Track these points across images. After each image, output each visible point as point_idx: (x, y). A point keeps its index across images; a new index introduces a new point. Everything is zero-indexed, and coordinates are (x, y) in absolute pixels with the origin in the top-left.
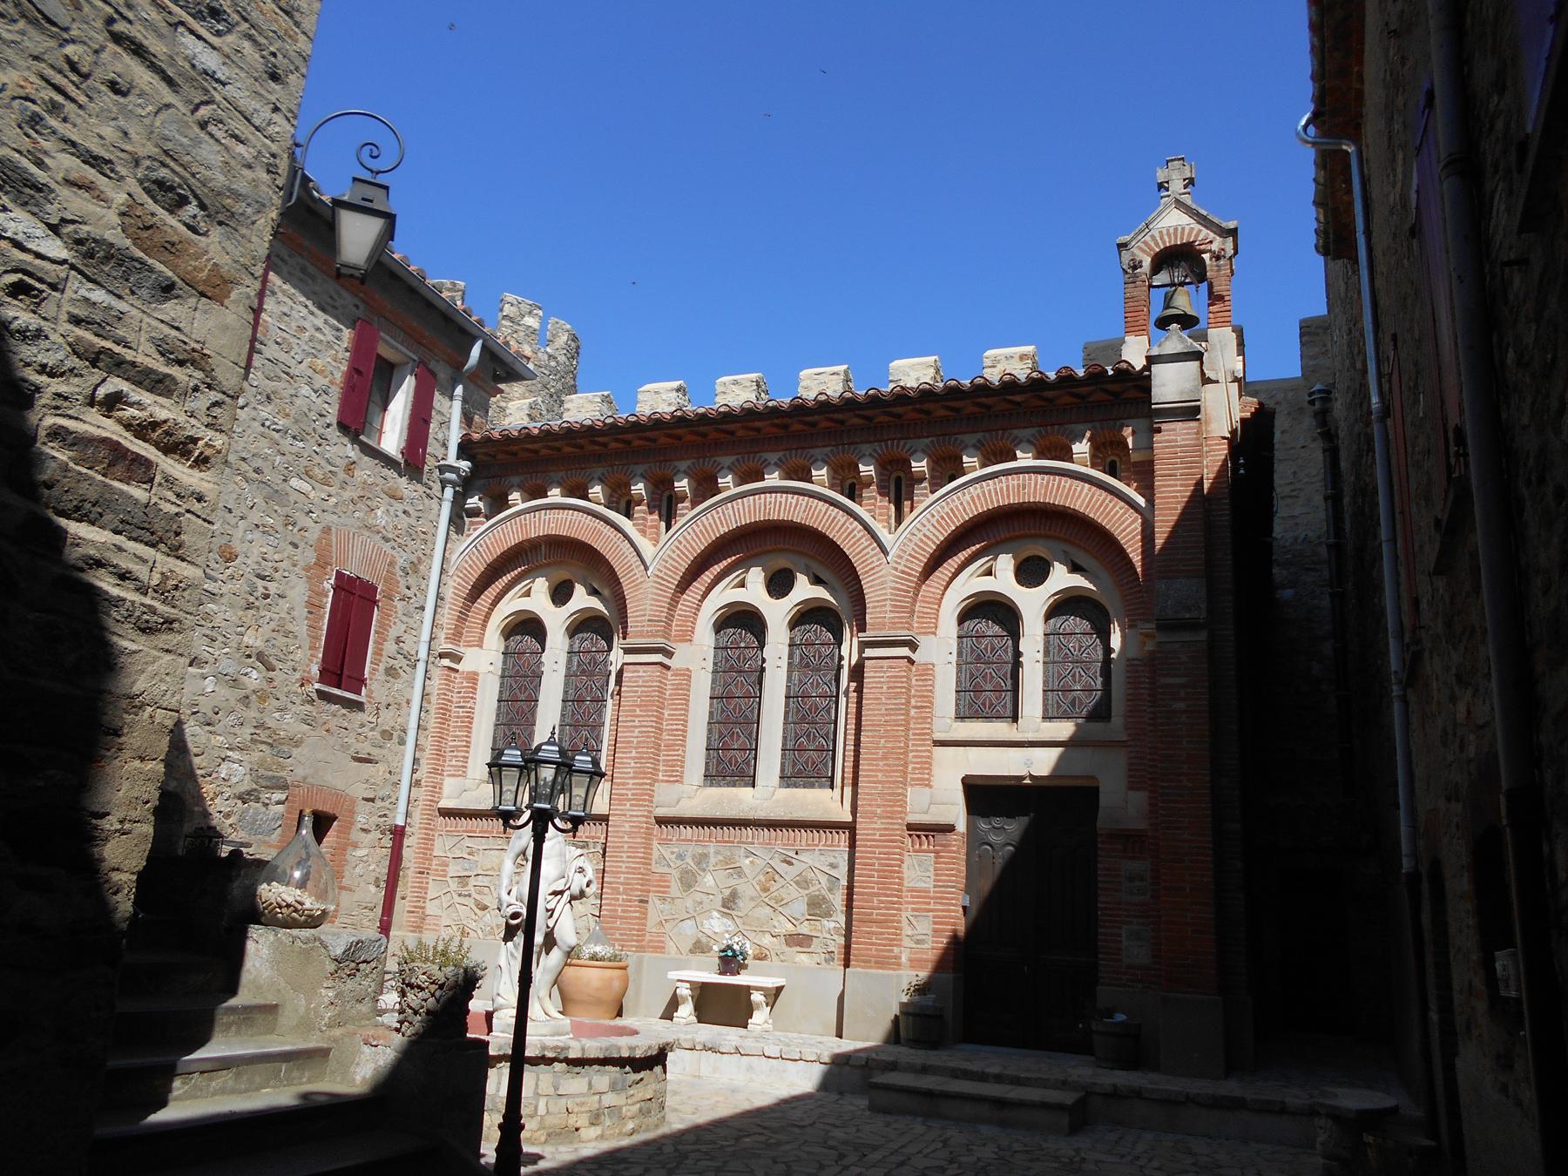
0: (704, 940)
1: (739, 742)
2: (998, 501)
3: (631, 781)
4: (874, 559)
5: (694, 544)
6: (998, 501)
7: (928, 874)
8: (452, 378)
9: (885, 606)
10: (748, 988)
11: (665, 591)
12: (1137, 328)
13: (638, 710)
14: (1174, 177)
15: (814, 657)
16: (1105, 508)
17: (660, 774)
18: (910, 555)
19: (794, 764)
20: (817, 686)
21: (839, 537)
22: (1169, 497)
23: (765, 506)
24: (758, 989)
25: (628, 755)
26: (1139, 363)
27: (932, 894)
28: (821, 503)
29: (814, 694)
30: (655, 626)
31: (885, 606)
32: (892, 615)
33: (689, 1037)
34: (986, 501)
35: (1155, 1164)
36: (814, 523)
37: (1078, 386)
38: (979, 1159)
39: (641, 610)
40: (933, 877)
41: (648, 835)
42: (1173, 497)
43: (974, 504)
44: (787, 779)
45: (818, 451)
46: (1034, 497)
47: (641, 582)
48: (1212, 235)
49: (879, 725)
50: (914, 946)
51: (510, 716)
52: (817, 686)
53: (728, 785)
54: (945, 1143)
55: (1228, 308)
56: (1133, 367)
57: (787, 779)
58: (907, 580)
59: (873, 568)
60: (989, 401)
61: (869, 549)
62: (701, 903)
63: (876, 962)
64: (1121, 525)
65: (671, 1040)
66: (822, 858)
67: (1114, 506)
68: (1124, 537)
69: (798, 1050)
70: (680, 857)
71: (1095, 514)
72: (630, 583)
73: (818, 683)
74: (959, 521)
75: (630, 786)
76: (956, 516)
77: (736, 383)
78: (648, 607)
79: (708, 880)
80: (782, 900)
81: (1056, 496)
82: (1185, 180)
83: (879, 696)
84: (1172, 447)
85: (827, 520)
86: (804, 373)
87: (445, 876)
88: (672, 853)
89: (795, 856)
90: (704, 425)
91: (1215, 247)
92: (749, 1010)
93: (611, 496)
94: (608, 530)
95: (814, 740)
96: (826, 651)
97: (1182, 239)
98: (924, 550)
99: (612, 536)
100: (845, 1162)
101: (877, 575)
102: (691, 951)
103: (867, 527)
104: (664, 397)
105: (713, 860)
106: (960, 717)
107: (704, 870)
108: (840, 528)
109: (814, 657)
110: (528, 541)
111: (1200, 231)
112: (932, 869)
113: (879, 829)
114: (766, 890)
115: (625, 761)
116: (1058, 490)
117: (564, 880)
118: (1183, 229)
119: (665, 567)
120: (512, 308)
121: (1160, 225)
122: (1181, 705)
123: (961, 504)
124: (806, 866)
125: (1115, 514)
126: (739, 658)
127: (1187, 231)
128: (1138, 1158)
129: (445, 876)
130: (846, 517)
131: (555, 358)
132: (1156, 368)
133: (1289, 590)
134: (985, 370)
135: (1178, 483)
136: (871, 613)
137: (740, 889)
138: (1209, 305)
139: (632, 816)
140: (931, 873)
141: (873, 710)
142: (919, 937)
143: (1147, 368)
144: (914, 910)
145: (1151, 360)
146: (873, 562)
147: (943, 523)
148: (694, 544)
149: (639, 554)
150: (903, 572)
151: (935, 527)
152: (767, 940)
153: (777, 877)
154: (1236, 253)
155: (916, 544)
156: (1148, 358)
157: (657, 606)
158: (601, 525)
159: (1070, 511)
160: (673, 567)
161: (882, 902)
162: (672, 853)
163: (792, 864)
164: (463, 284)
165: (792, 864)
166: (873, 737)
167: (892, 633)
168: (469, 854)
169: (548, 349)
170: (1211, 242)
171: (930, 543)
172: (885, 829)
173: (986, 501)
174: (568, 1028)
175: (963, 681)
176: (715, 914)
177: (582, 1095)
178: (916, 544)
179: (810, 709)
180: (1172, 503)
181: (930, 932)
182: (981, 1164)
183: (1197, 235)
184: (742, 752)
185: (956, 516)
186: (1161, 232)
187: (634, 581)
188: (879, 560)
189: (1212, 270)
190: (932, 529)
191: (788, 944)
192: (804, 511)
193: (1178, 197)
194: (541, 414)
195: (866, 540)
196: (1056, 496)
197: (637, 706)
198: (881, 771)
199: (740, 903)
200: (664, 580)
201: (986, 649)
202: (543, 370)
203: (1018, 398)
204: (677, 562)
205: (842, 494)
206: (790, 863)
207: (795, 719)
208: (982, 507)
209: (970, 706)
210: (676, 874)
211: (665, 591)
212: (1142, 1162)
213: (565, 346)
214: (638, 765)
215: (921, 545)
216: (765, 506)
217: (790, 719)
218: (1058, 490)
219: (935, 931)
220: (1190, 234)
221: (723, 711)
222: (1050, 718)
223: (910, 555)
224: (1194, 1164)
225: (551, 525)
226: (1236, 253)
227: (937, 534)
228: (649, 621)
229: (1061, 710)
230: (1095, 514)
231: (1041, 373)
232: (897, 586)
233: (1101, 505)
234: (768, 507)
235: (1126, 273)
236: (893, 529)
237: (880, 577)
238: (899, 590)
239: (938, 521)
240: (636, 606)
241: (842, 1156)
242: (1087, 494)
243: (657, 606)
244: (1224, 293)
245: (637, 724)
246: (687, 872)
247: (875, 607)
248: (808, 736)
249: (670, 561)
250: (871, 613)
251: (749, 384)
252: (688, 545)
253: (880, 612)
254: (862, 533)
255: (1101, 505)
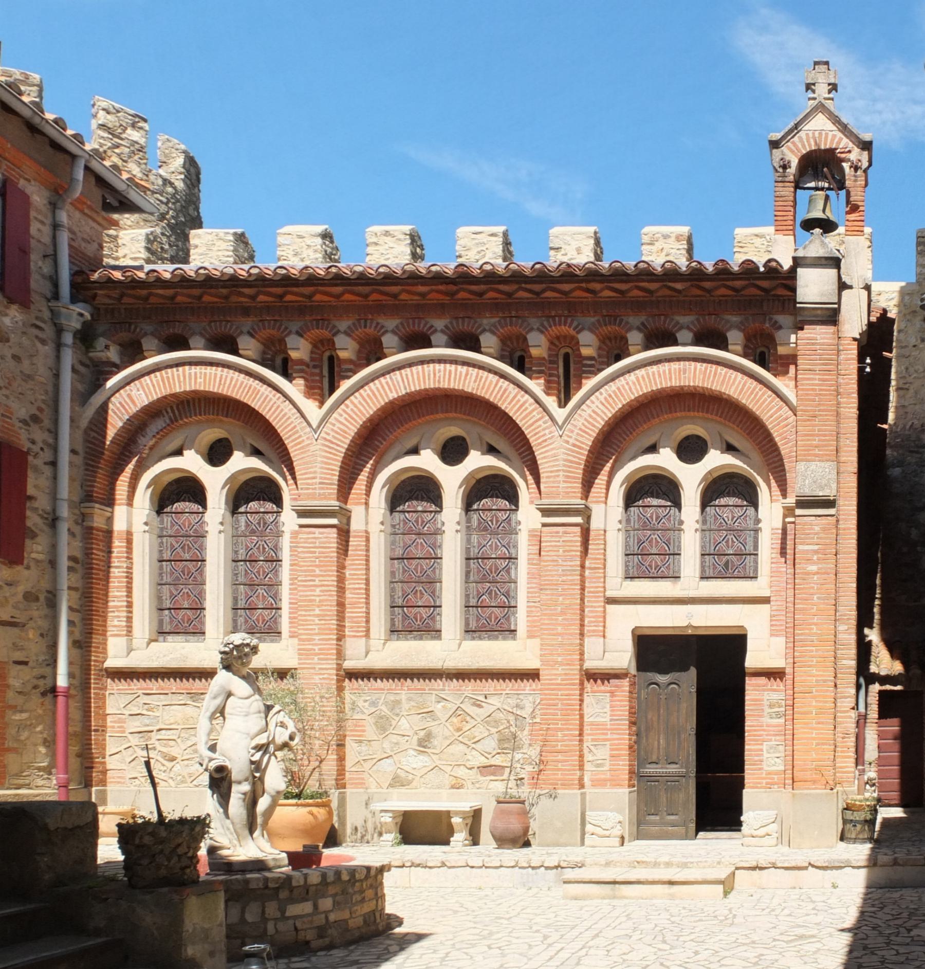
0: (402, 774)
1: (424, 599)
2: (661, 383)
3: (317, 638)
4: (547, 431)
5: (362, 408)
6: (661, 383)
7: (605, 710)
8: (50, 203)
9: (558, 476)
10: (448, 812)
11: (334, 454)
12: (784, 228)
13: (317, 570)
14: (820, 81)
15: (491, 521)
16: (756, 395)
17: (347, 630)
18: (580, 429)
19: (478, 620)
20: (496, 549)
21: (511, 409)
22: (808, 390)
23: (435, 374)
24: (457, 813)
25: (312, 613)
26: (787, 264)
27: (609, 727)
28: (491, 376)
29: (493, 556)
30: (327, 488)
31: (558, 476)
32: (566, 485)
33: (398, 856)
34: (650, 382)
35: (786, 912)
36: (486, 393)
37: (733, 280)
38: (656, 926)
39: (311, 473)
40: (609, 713)
41: (340, 689)
42: (812, 390)
43: (640, 384)
44: (470, 632)
45: (485, 321)
46: (694, 382)
47: (309, 445)
48: (851, 145)
49: (556, 585)
50: (594, 769)
51: (174, 576)
52: (496, 549)
53: (415, 638)
54: (628, 917)
55: (862, 218)
56: (781, 267)
57: (470, 632)
58: (577, 453)
59: (545, 441)
60: (653, 286)
61: (540, 422)
62: (397, 743)
63: (562, 785)
64: (768, 412)
65: (385, 863)
66: (509, 700)
67: (763, 395)
68: (771, 423)
69: (498, 859)
70: (374, 704)
71: (747, 400)
72: (296, 445)
73: (497, 546)
74: (625, 399)
75: (317, 642)
76: (623, 395)
77: (387, 233)
78: (319, 470)
79: (404, 724)
80: (474, 737)
81: (713, 382)
82: (829, 84)
83: (555, 558)
84: (813, 344)
85: (498, 392)
86: (462, 231)
87: (124, 732)
88: (365, 701)
89: (483, 699)
90: (362, 285)
91: (853, 156)
92: (451, 831)
93: (264, 353)
94: (265, 389)
95: (496, 598)
96: (502, 516)
97: (826, 144)
98: (594, 426)
99: (271, 396)
100: (549, 941)
101: (551, 447)
102: (391, 786)
103: (538, 401)
104: (309, 243)
105: (405, 705)
106: (629, 577)
107: (397, 715)
108: (512, 401)
109: (491, 521)
110: (174, 395)
111: (841, 139)
112: (608, 706)
113: (560, 675)
114: (459, 730)
115: (309, 618)
116: (714, 377)
117: (266, 734)
118: (827, 135)
119: (332, 430)
120: (109, 117)
121: (806, 128)
122: (814, 568)
123: (627, 383)
124: (495, 708)
125: (764, 402)
126: (417, 521)
127: (830, 137)
128: (773, 910)
129: (124, 732)
130: (517, 389)
131: (171, 184)
132: (800, 271)
133: (897, 469)
134: (644, 247)
135: (817, 377)
136: (545, 483)
137: (435, 730)
138: (847, 213)
139: (321, 669)
140: (607, 709)
141: (550, 571)
142: (599, 762)
143: (793, 270)
144: (593, 740)
145: (798, 262)
146: (545, 435)
147: (611, 401)
148: (362, 408)
149: (303, 415)
150: (574, 445)
151: (603, 404)
152: (462, 772)
153: (468, 718)
154: (870, 165)
155: (586, 420)
156: (795, 259)
157: (328, 469)
158: (256, 384)
159: (725, 396)
160: (341, 429)
161: (565, 735)
162: (365, 701)
163: (482, 707)
164: (37, 77)
165: (482, 707)
166: (552, 595)
167: (566, 501)
168: (148, 710)
169: (161, 172)
170: (850, 152)
171: (599, 419)
172: (566, 674)
173: (650, 382)
174: (286, 862)
175: (631, 544)
176: (412, 752)
177: (308, 915)
178: (586, 420)
179: (490, 569)
180: (811, 395)
181: (607, 757)
182: (658, 928)
183: (839, 143)
184: (427, 609)
185: (623, 395)
186: (807, 135)
187: (299, 443)
188: (551, 433)
189: (850, 180)
190: (601, 406)
191: (482, 774)
192: (475, 381)
193: (823, 101)
194: (162, 248)
195: (538, 414)
196: (713, 382)
197: (316, 566)
198: (560, 625)
199: (435, 742)
200: (333, 443)
201: (651, 517)
202: (156, 196)
203: (679, 286)
204: (344, 425)
205: (512, 366)
206: (480, 706)
207: (476, 578)
208: (646, 387)
209: (639, 567)
210: (371, 720)
211: (334, 454)
212: (777, 912)
213: (183, 170)
214: (323, 622)
215: (591, 420)
216: (435, 374)
217: (472, 578)
218: (714, 377)
219: (612, 756)
220: (832, 140)
221: (404, 571)
222: (707, 578)
223: (580, 429)
224: (814, 909)
225: (199, 380)
226: (870, 165)
227: (606, 411)
228: (321, 483)
229: (717, 571)
230: (747, 400)
231: (699, 263)
232: (570, 458)
233: (752, 393)
234: (437, 375)
235: (776, 171)
236: (563, 403)
237: (552, 449)
238: (571, 462)
239: (605, 399)
240: (304, 469)
241: (546, 937)
242: (740, 382)
243: (328, 469)
244: (860, 204)
245: (317, 583)
246: (381, 718)
247: (547, 477)
248: (490, 594)
249: (338, 425)
250: (545, 483)
251: (402, 237)
252: (355, 409)
253: (554, 482)
254: (533, 407)
255: (752, 393)
